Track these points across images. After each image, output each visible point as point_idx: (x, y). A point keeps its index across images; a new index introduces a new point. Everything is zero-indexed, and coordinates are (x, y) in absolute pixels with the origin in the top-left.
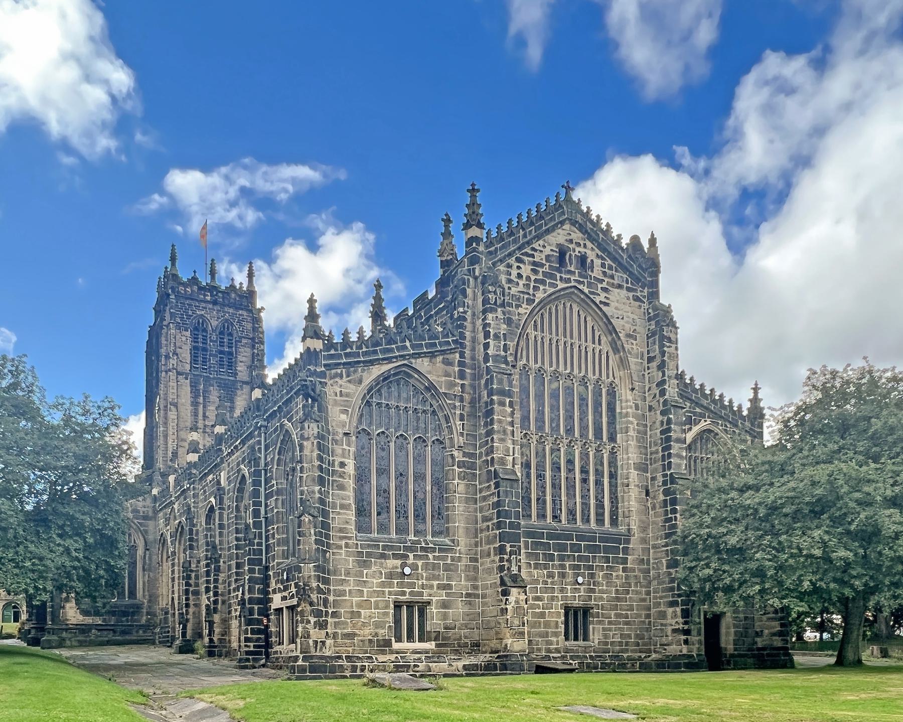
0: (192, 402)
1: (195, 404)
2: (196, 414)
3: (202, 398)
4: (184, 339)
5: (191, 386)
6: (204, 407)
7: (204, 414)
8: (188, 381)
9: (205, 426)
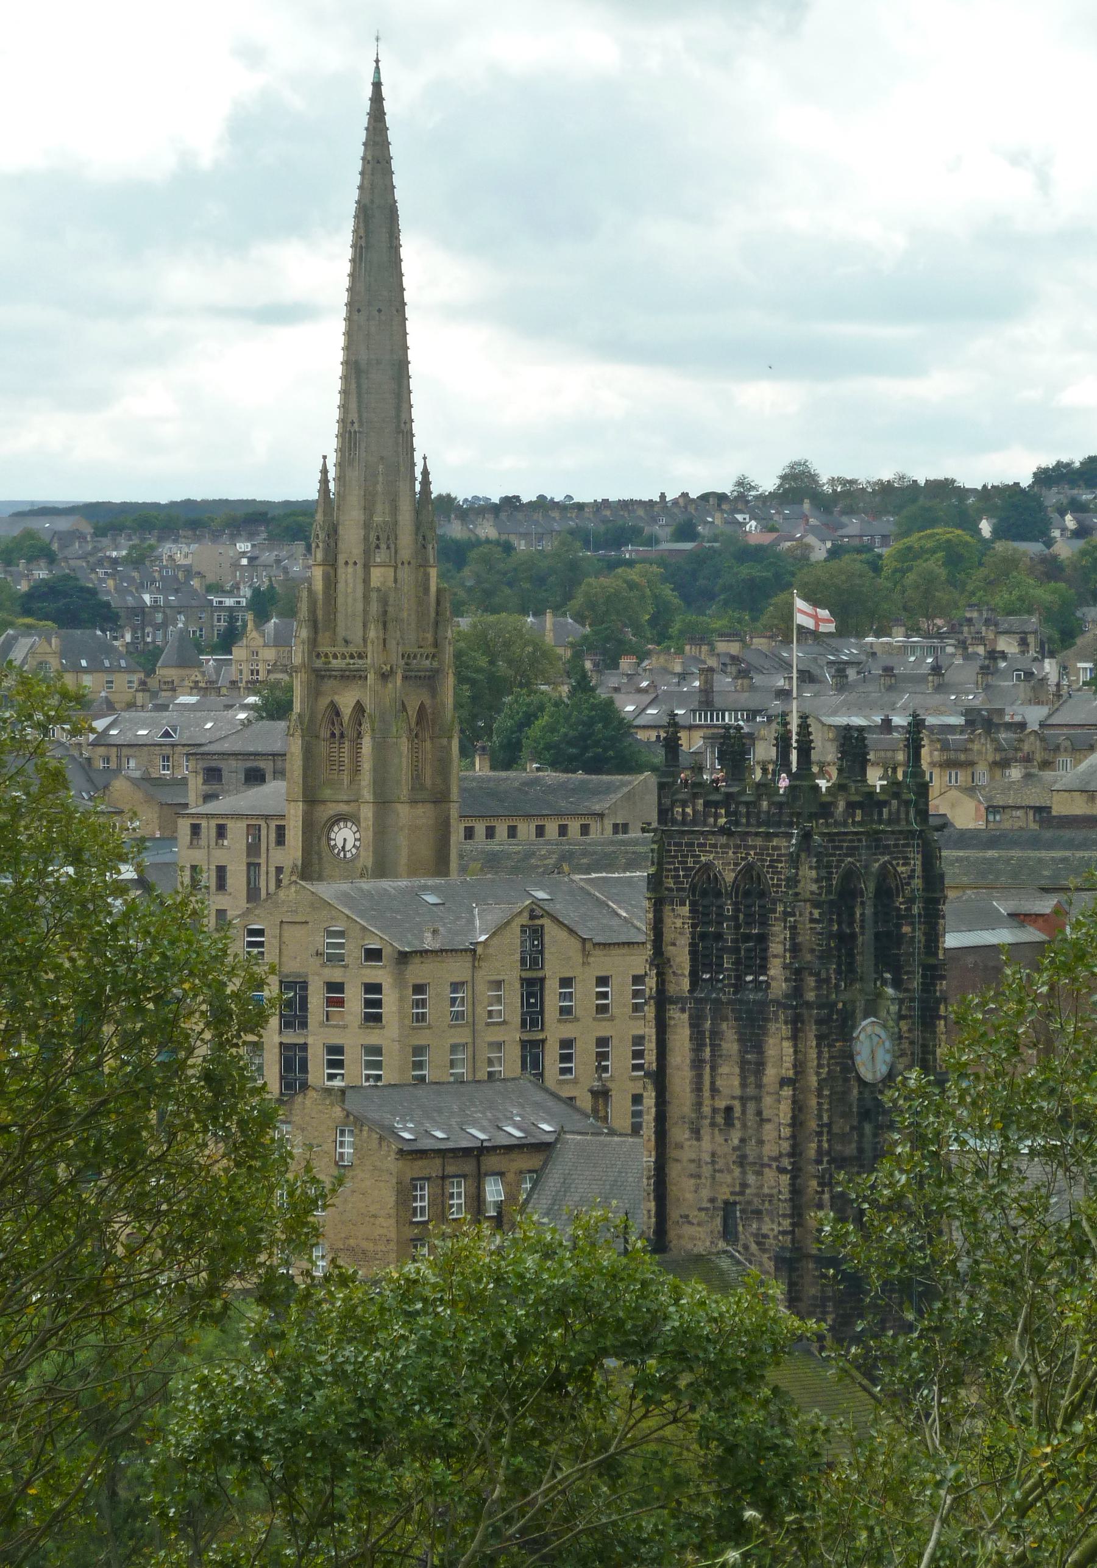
0: (693, 1061)
1: (697, 1064)
2: (698, 1089)
3: (708, 1049)
4: (679, 923)
5: (691, 1026)
6: (713, 1068)
7: (713, 1083)
8: (686, 1016)
9: (715, 1110)
